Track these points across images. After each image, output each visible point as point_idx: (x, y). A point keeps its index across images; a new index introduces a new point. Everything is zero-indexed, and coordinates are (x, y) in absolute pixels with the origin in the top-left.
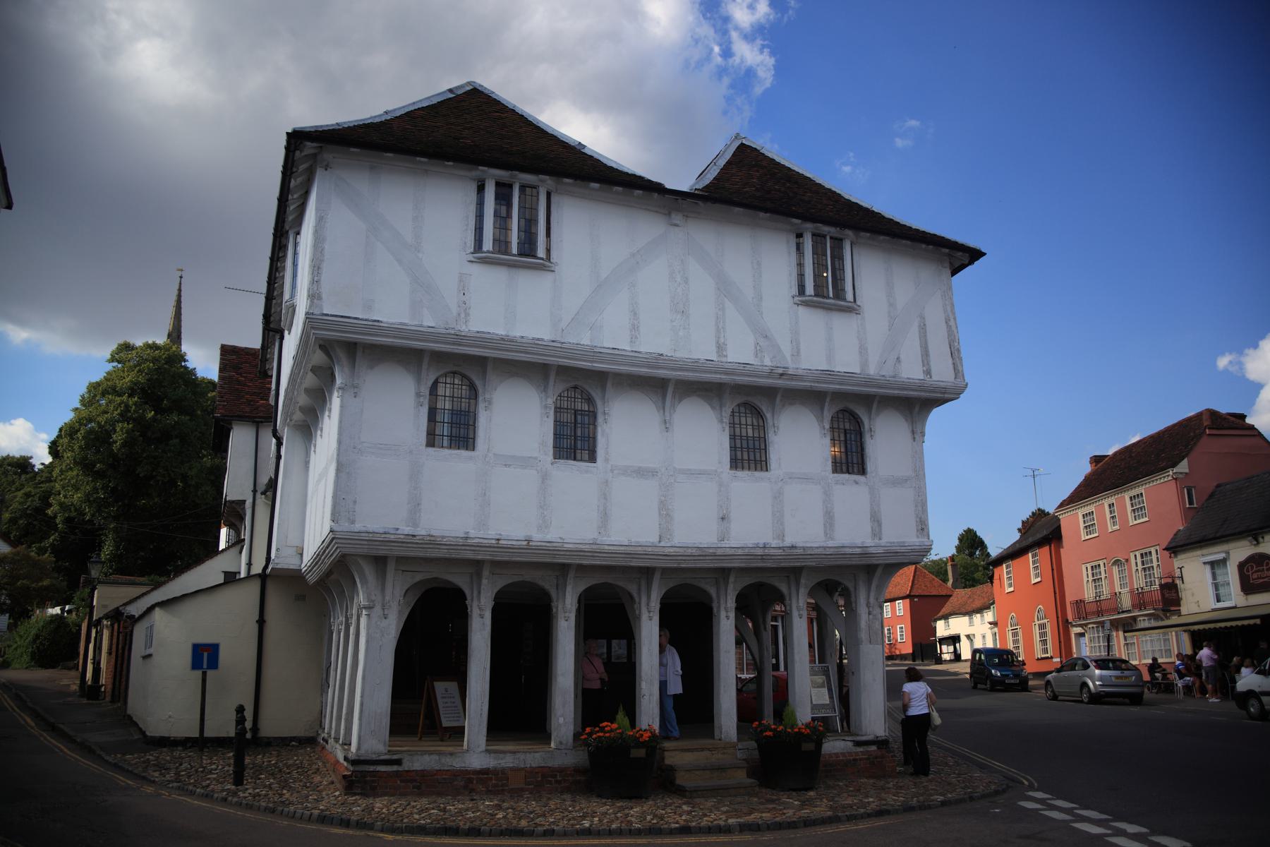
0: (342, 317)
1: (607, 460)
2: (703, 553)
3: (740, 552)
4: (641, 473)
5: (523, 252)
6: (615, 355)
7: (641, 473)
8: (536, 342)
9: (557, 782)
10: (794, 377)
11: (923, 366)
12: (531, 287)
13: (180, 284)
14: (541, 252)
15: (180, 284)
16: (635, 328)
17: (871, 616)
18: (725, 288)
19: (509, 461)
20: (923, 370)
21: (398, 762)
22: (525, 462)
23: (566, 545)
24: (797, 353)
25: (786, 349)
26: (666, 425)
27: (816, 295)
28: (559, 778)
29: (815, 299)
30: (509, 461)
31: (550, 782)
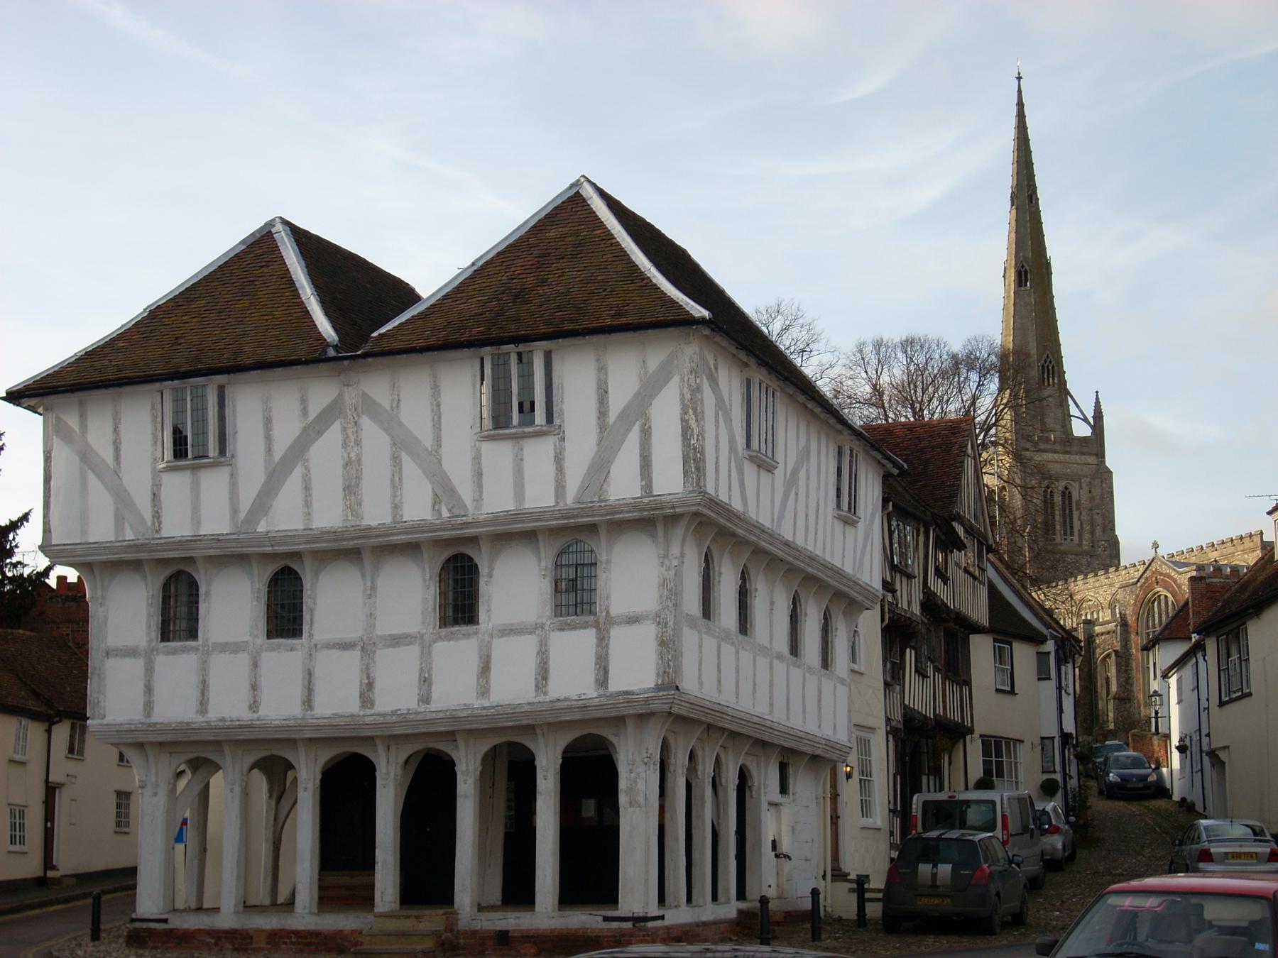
0: (64, 545)
1: (311, 635)
2: (404, 718)
3: (441, 715)
4: (345, 646)
5: (196, 455)
6: (289, 537)
7: (345, 646)
8: (216, 539)
9: (292, 943)
10: (477, 524)
11: (642, 480)
12: (214, 483)
13: (1020, 92)
14: (213, 451)
15: (1020, 92)
16: (308, 503)
17: (633, 775)
18: (402, 443)
19: (226, 648)
20: (642, 486)
21: (165, 921)
22: (235, 648)
23: (274, 722)
24: (478, 499)
25: (466, 492)
26: (372, 592)
27: (495, 428)
28: (294, 940)
29: (492, 432)
30: (226, 648)
31: (285, 943)
